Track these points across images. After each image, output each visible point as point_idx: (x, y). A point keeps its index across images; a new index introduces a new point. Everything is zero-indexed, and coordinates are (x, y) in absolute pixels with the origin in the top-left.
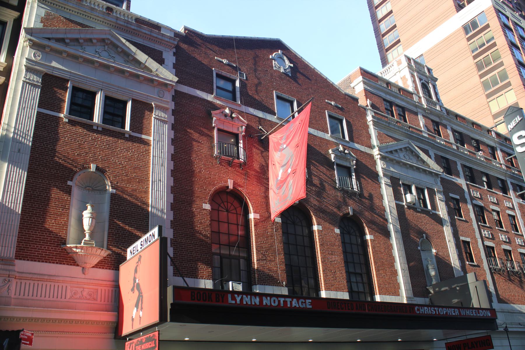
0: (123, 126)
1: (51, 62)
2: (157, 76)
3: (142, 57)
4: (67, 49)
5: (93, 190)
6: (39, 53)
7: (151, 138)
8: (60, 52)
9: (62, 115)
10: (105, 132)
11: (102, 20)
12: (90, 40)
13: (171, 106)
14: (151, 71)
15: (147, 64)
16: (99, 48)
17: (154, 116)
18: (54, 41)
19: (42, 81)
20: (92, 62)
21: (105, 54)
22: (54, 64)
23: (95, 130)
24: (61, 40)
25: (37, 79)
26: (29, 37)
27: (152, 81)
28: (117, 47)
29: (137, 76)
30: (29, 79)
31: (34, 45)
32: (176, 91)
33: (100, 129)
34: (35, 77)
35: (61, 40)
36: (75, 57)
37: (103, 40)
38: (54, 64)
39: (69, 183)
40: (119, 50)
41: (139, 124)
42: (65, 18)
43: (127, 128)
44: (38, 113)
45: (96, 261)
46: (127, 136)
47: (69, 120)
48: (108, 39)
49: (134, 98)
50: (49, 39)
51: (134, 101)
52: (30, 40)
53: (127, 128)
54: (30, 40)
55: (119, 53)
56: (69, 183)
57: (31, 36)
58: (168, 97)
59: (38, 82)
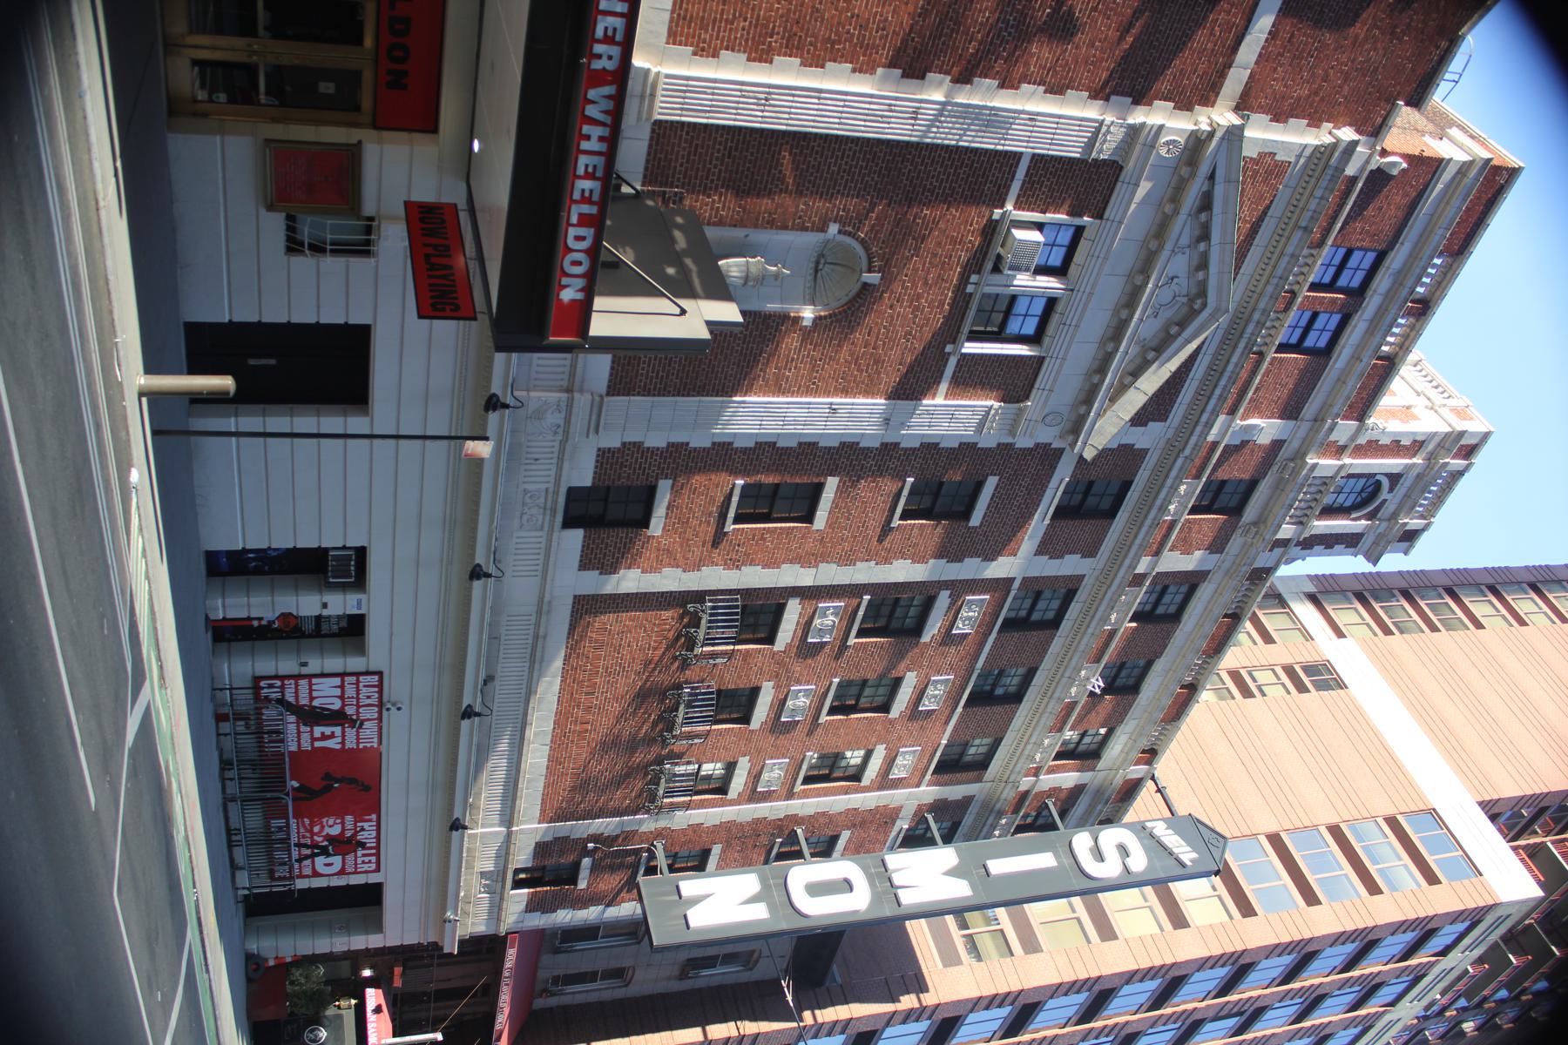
0: (975, 336)
2: (1098, 415)
3: (1151, 382)
4: (1182, 217)
5: (816, 271)
6: (1176, 152)
7: (939, 400)
8: (1175, 198)
9: (1009, 207)
10: (961, 301)
12: (1203, 265)
13: (1023, 442)
14: (1113, 400)
16: (1183, 285)
17: (996, 405)
18: (1205, 188)
20: (1145, 268)
21: (1166, 295)
25: (1105, 150)
26: (1219, 135)
27: (1088, 398)
28: (1182, 324)
29: (1102, 370)
30: (1108, 132)
31: (1197, 142)
32: (1061, 451)
33: (970, 289)
34: (1114, 145)
35: (1206, 204)
37: (1202, 293)
39: (833, 229)
41: (975, 375)
42: (1268, 207)
43: (971, 348)
44: (1017, 156)
46: (949, 348)
48: (1204, 305)
50: (1212, 177)
51: (1040, 361)
53: (971, 348)
54: (1211, 134)
55: (1166, 329)
56: (833, 229)
57: (1222, 139)
58: (1048, 435)
59: (1101, 151)
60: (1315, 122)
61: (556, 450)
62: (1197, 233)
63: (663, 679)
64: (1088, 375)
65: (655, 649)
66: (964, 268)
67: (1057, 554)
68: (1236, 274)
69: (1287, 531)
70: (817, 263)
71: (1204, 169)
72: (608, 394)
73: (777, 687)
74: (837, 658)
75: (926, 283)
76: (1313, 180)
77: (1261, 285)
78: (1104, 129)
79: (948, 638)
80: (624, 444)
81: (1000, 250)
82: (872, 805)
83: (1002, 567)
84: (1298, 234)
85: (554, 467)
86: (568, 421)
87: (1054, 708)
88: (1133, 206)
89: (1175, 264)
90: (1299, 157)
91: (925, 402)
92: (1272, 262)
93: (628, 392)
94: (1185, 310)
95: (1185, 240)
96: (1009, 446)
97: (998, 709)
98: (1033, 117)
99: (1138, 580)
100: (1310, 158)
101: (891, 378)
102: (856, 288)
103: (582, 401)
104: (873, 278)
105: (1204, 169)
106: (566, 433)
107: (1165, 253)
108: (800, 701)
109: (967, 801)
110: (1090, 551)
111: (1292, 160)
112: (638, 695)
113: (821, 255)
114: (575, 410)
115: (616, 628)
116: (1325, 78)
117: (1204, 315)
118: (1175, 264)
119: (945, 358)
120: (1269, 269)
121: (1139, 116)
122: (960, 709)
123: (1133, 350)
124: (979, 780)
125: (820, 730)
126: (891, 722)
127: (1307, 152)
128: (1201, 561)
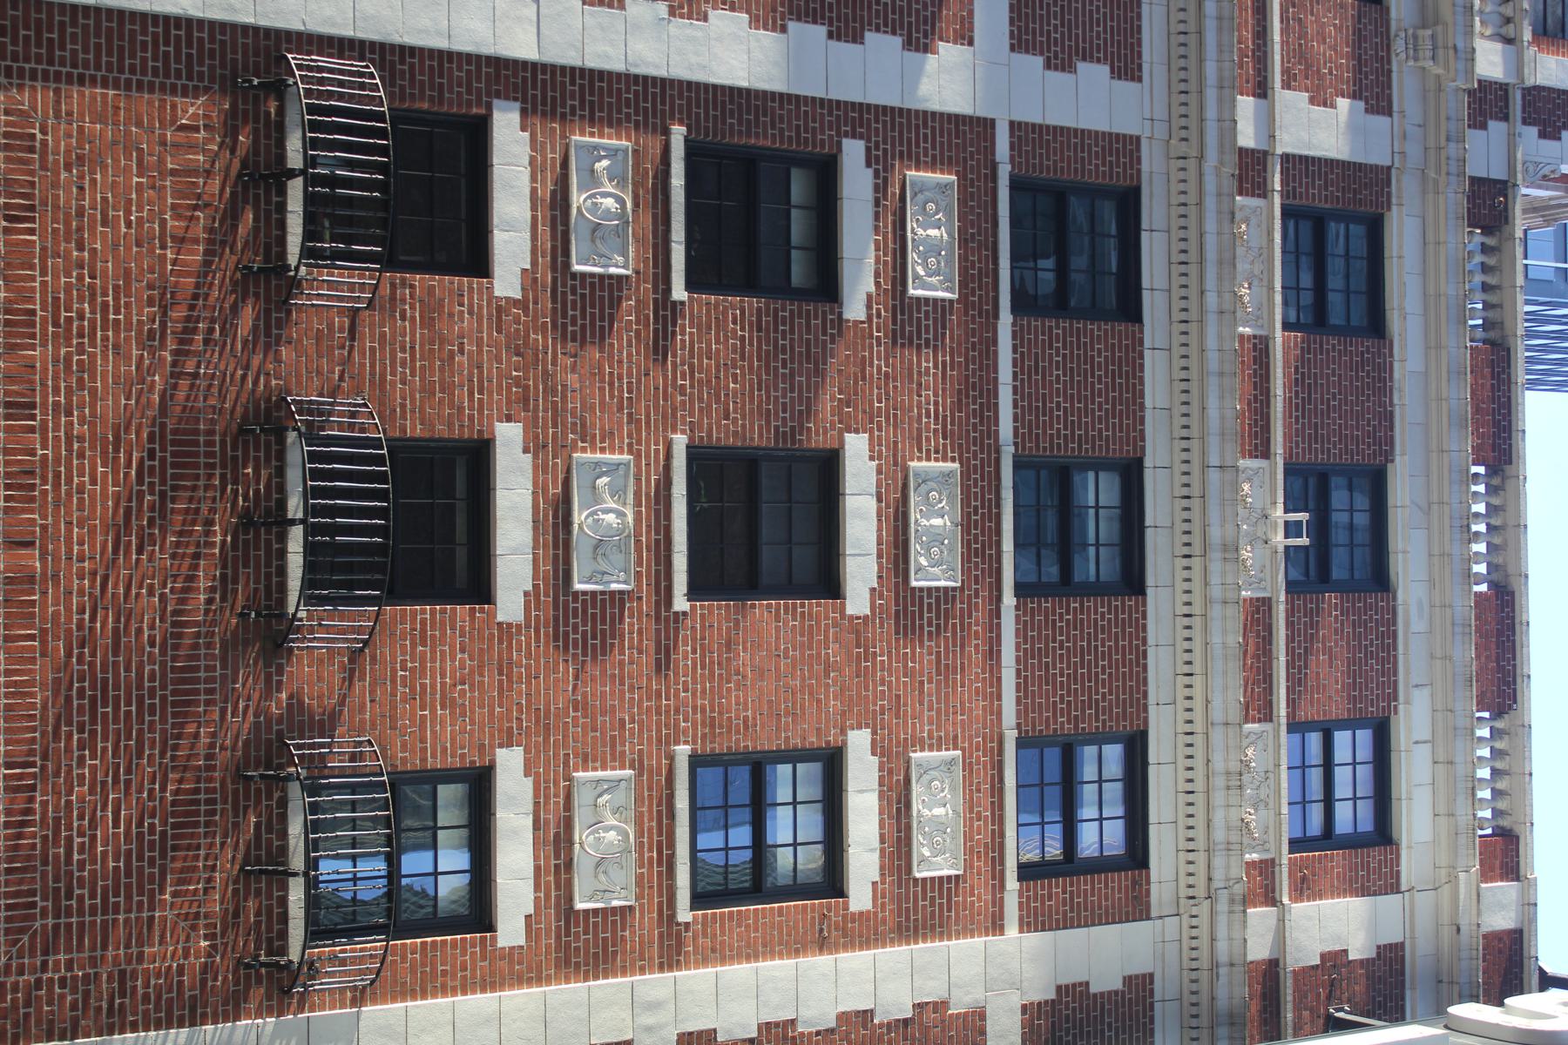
63: (225, 377)
65: (180, 241)
67: (1060, 62)
69: (1490, 62)
73: (533, 445)
74: (660, 348)
79: (905, 318)
82: (895, 1002)
83: (946, 80)
87: (1227, 633)
97: (1098, 610)
99: (1251, 170)
108: (604, 514)
109: (1140, 987)
110: (1127, 67)
112: (158, 435)
115: (60, 142)
122: (1009, 600)
124: (1138, 908)
125: (685, 654)
126: (858, 626)
128: (1353, 128)
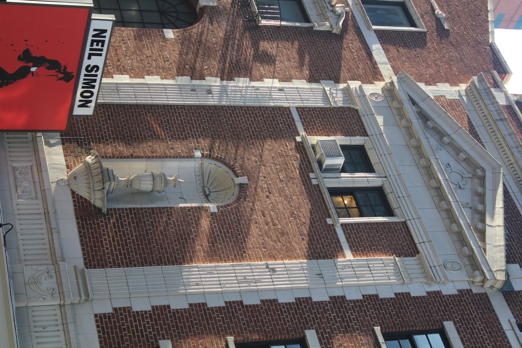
1: (379, 114)
11: (513, 161)
12: (457, 150)
15: (488, 229)
19: (340, 108)
22: (380, 120)
23: (308, 176)
24: (424, 117)
28: (483, 185)
31: (389, 91)
34: (341, 99)
35: (424, 117)
36: (409, 130)
38: (380, 120)
40: (462, 156)
42: (470, 122)
45: (83, 192)
47: (302, 143)
48: (484, 170)
49: (408, 222)
50: (414, 103)
52: (392, 83)
59: (335, 102)
60: (454, 83)
61: (59, 317)
62: (437, 137)
64: (449, 231)
66: (301, 169)
68: (479, 140)
70: (204, 192)
71: (403, 97)
72: (87, 268)
75: (281, 181)
76: (480, 101)
77: (511, 158)
78: (328, 92)
80: (115, 309)
81: (318, 156)
84: (500, 124)
85: (61, 333)
86: (60, 284)
88: (382, 128)
89: (440, 159)
90: (460, 96)
91: (339, 260)
92: (504, 145)
93: (102, 264)
94: (476, 181)
95: (434, 142)
96: (438, 294)
98: (281, 90)
100: (467, 95)
101: (301, 245)
102: (236, 190)
103: (65, 267)
104: (244, 180)
105: (403, 97)
106: (62, 294)
107: (433, 161)
111: (458, 98)
113: (203, 187)
114: (62, 273)
116: (437, 65)
117: (489, 175)
118: (440, 159)
119: (331, 228)
120: (506, 148)
121: (342, 86)
123: (467, 213)
127: (463, 93)
